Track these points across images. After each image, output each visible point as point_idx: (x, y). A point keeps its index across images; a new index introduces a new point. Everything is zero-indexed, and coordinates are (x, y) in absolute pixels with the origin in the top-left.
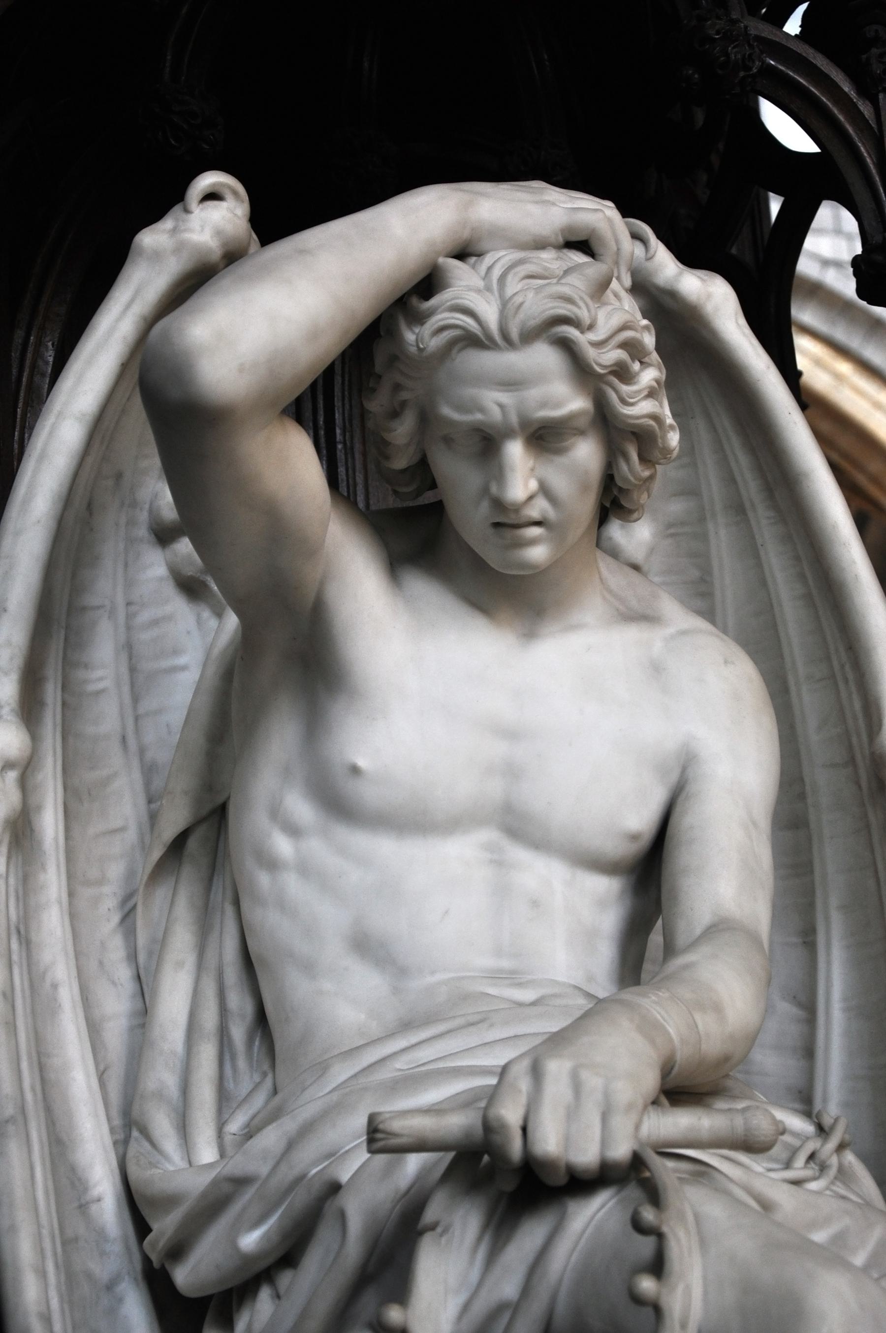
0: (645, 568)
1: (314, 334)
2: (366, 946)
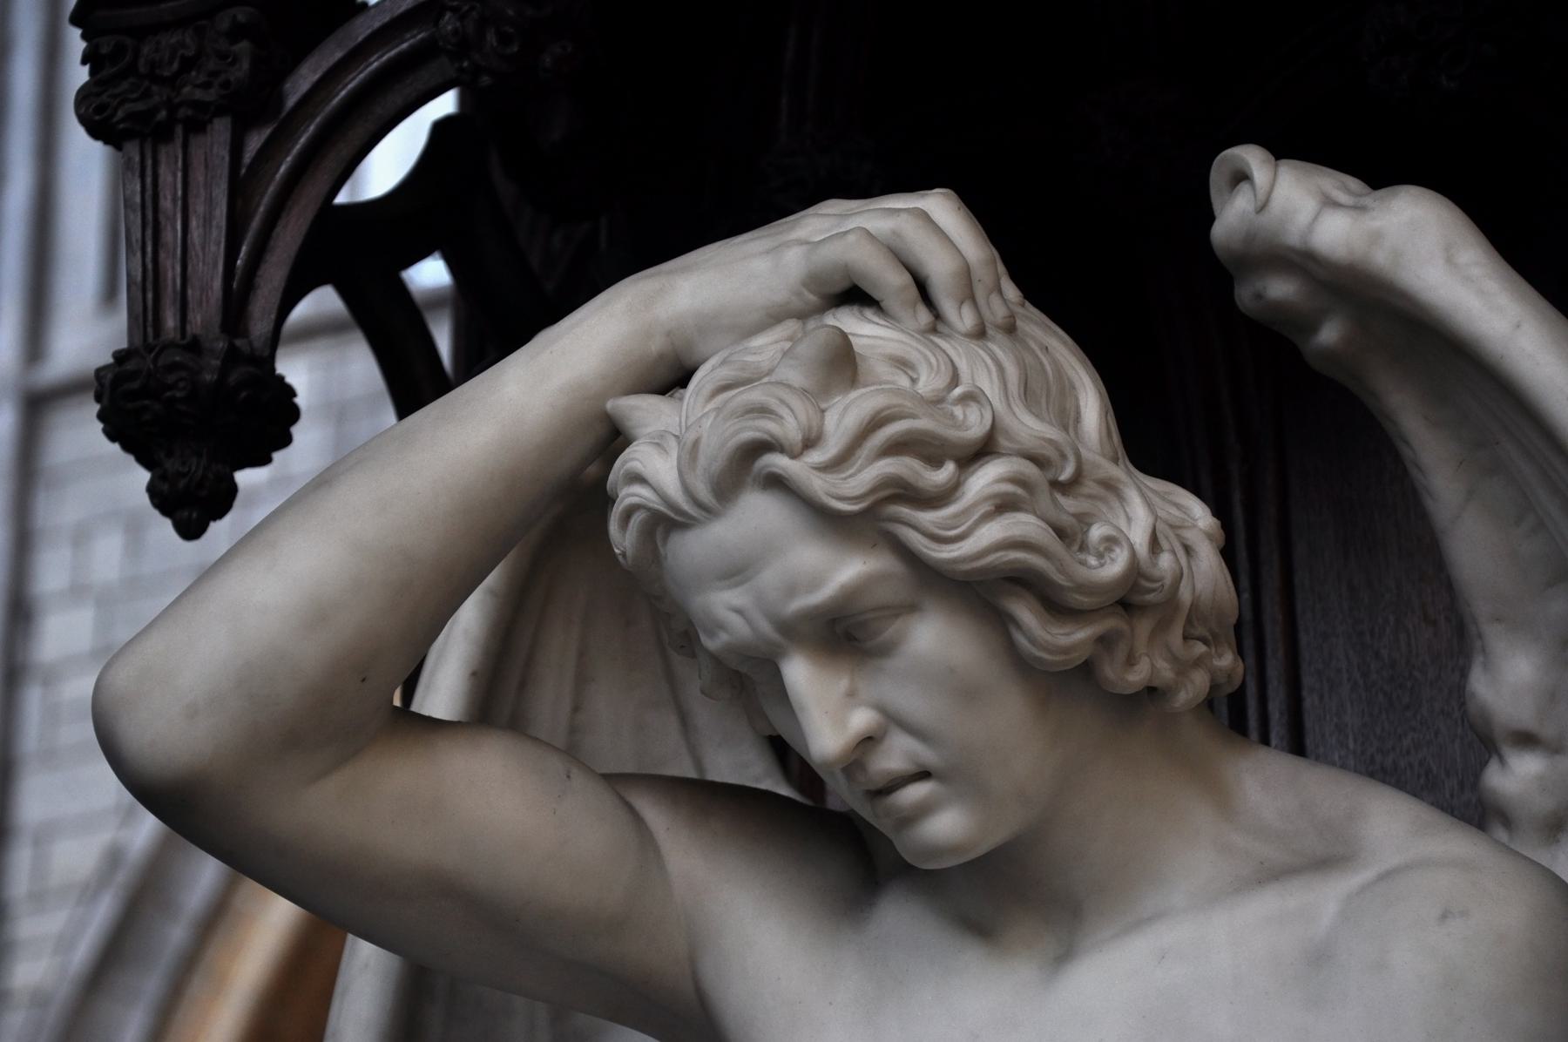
0: (1548, 731)
1: (318, 615)
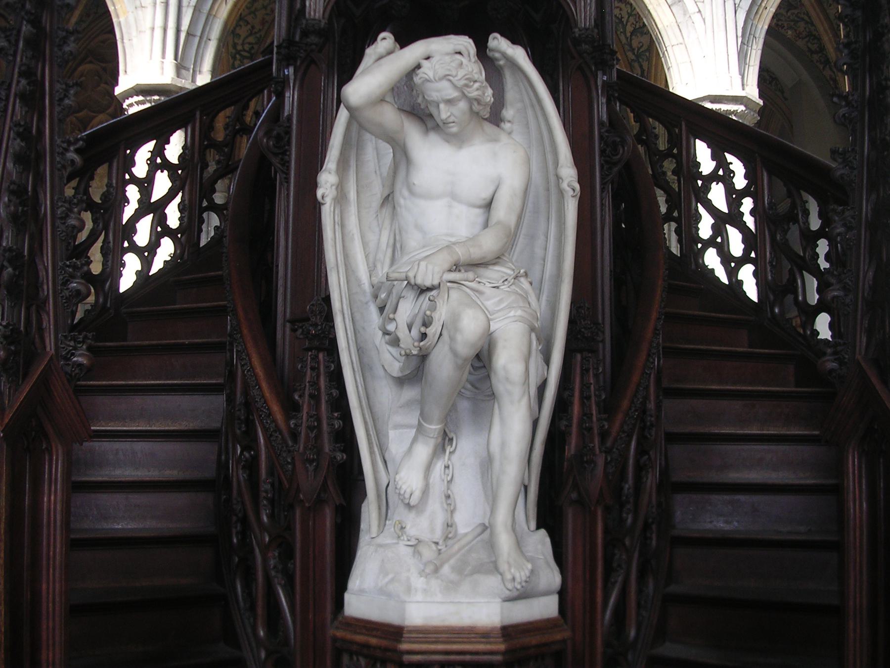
2: (418, 227)
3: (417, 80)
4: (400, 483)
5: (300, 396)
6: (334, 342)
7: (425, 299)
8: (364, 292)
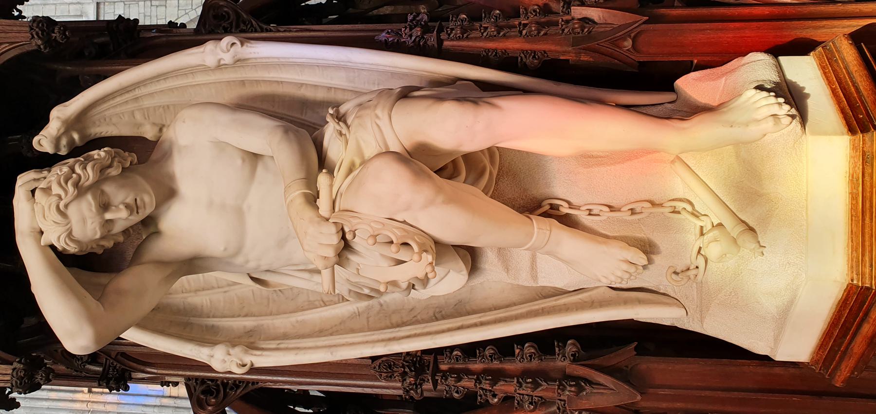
3: (72, 249)
4: (613, 278)
5: (494, 396)
6: (425, 352)
7: (358, 243)
8: (368, 308)
